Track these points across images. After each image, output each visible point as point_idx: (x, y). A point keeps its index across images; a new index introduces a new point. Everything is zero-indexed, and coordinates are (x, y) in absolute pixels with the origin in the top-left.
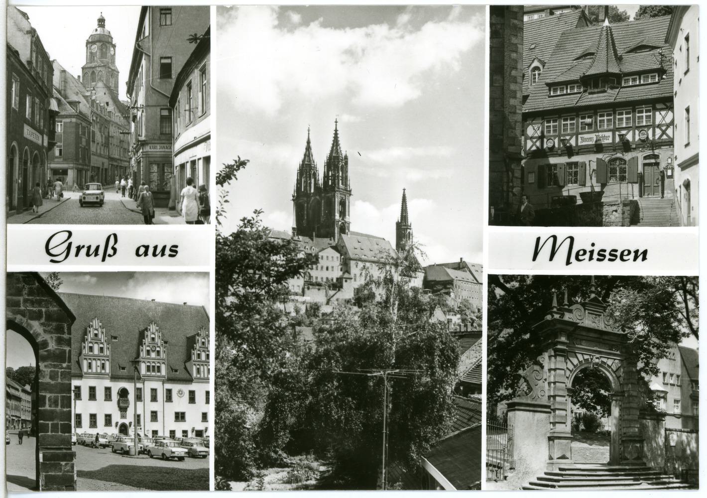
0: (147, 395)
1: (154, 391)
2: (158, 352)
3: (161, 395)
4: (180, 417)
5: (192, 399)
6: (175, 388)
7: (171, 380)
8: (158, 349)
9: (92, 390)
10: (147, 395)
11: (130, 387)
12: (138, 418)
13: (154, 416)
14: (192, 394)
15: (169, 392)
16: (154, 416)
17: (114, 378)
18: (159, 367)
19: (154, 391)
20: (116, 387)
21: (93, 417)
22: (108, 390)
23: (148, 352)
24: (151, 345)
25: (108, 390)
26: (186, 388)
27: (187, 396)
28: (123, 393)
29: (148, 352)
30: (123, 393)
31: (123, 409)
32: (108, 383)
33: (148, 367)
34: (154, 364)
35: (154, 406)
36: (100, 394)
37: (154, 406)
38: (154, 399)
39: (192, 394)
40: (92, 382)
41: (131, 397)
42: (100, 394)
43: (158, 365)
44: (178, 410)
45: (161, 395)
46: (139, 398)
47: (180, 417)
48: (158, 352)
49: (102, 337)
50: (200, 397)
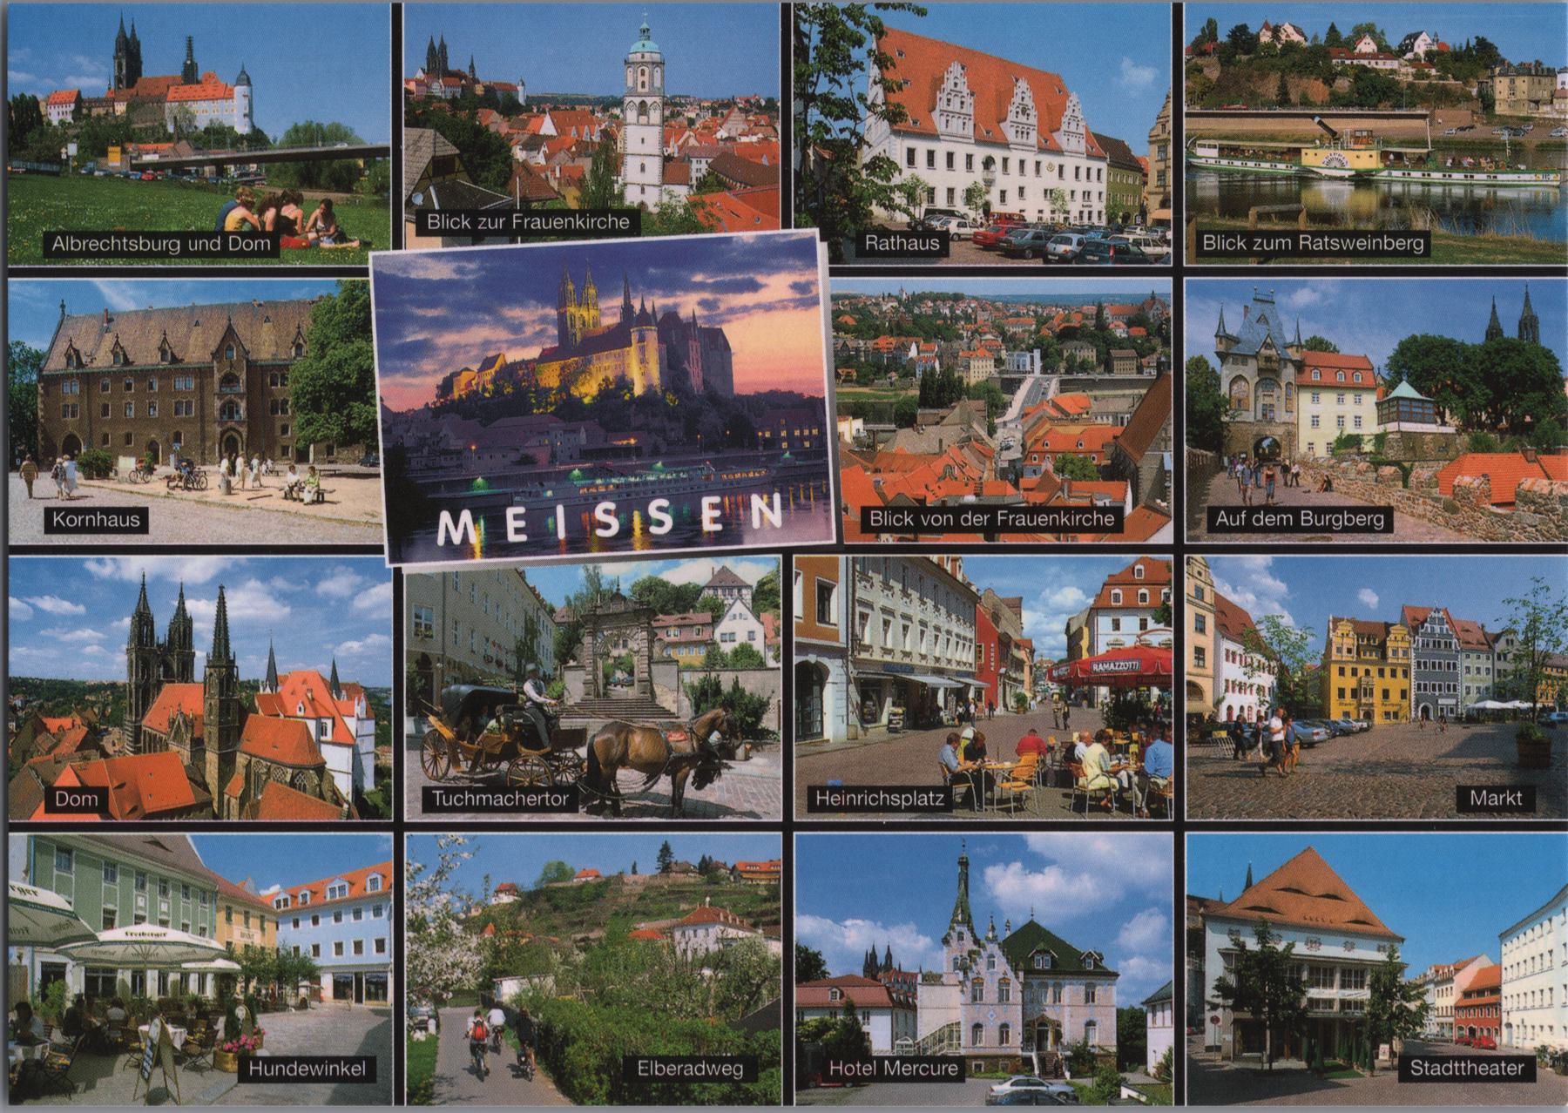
0: (1014, 165)
1: (1022, 162)
3: (1030, 167)
4: (1048, 193)
7: (1042, 150)
9: (950, 156)
11: (998, 155)
12: (1003, 193)
13: (1021, 190)
14: (1061, 167)
15: (1038, 164)
16: (1021, 190)
17: (980, 142)
19: (1022, 162)
20: (980, 154)
22: (969, 157)
25: (969, 157)
26: (1056, 160)
28: (988, 163)
31: (989, 183)
32: (973, 149)
37: (1022, 181)
39: (1061, 167)
45: (1030, 167)
49: (966, 91)
50: (1069, 172)
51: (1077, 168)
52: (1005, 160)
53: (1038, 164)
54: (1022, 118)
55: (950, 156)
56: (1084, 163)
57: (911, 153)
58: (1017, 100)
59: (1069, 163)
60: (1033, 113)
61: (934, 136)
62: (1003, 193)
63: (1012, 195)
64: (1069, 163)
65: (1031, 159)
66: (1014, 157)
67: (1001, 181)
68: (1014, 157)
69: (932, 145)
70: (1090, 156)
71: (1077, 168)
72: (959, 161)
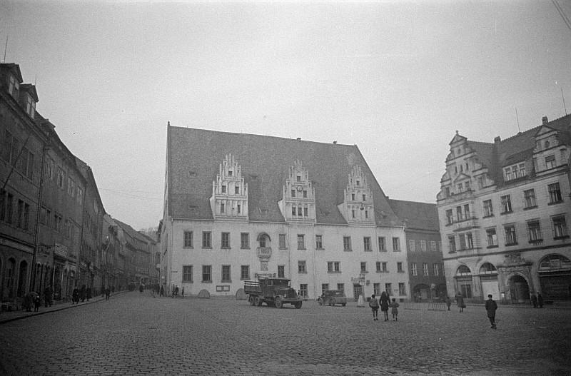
0: (293, 241)
3: (310, 241)
4: (334, 267)
10: (293, 241)
11: (272, 230)
14: (347, 240)
17: (252, 220)
18: (306, 209)
20: (254, 231)
21: (226, 269)
22: (245, 236)
23: (293, 191)
25: (245, 236)
28: (263, 238)
30: (263, 238)
33: (294, 209)
38: (301, 247)
39: (347, 240)
41: (274, 244)
45: (310, 241)
46: (283, 246)
47: (334, 267)
50: (357, 243)
51: (367, 240)
52: (282, 236)
53: (319, 236)
54: (300, 196)
55: (225, 236)
56: (374, 234)
57: (188, 236)
58: (293, 180)
59: (357, 236)
60: (309, 190)
61: (210, 218)
68: (292, 235)
69: (205, 227)
70: (379, 226)
71: (367, 240)
72: (235, 240)
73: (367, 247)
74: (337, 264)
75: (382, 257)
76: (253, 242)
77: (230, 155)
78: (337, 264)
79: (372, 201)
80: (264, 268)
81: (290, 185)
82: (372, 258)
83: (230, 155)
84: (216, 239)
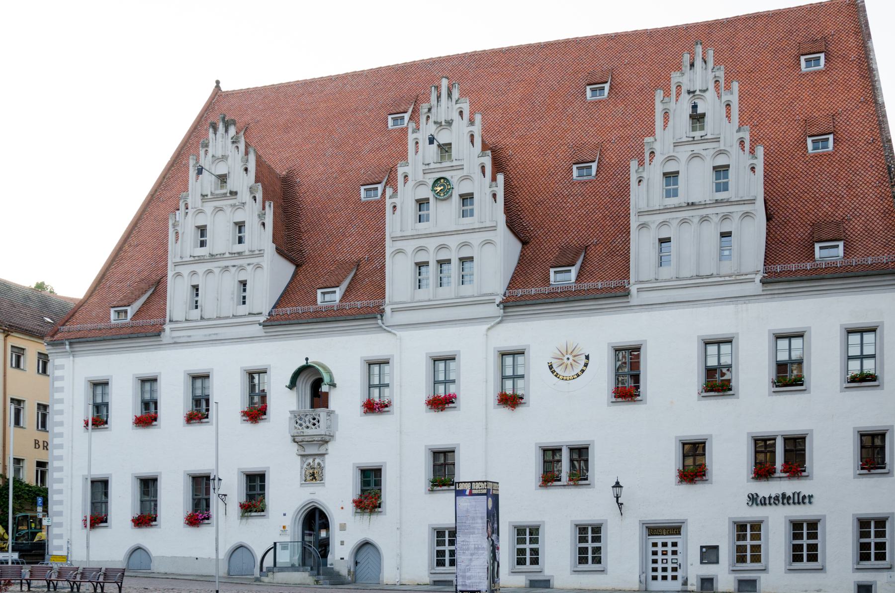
2: (467, 198)
4: (565, 465)
5: (628, 386)
6: (543, 335)
8: (465, 188)
24: (430, 179)
27: (601, 375)
29: (422, 203)
34: (443, 256)
35: (441, 430)
36: (229, 398)
40: (198, 359)
42: (229, 398)
43: (465, 253)
44: (552, 440)
48: (467, 198)
54: (445, 214)
56: (755, 324)
59: (669, 335)
62: (370, 489)
63: (406, 481)
64: (669, 335)
65: (476, 348)
66: (408, 351)
67: (355, 439)
73: (717, 383)
74: (580, 454)
75: (782, 416)
76: (284, 402)
77: (699, 49)
78: (580, 454)
79: (757, 190)
80: (314, 476)
81: (411, 183)
82: (731, 430)
83: (699, 49)
84: (173, 402)
